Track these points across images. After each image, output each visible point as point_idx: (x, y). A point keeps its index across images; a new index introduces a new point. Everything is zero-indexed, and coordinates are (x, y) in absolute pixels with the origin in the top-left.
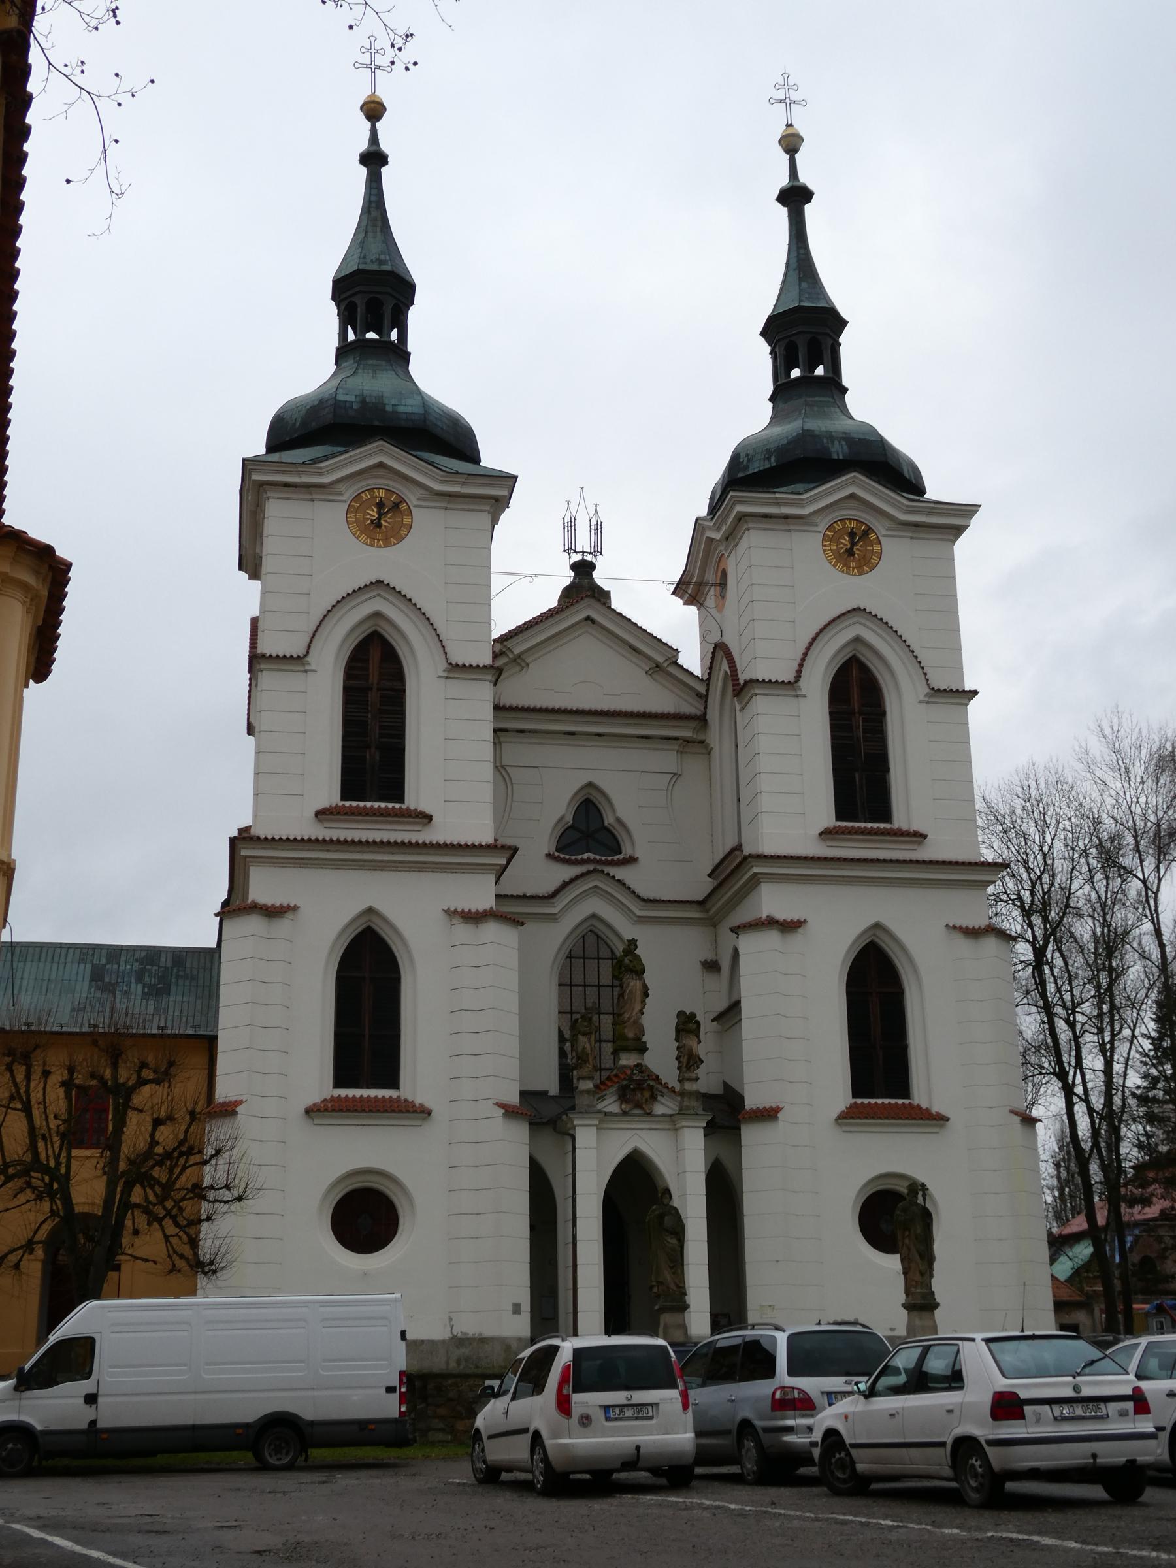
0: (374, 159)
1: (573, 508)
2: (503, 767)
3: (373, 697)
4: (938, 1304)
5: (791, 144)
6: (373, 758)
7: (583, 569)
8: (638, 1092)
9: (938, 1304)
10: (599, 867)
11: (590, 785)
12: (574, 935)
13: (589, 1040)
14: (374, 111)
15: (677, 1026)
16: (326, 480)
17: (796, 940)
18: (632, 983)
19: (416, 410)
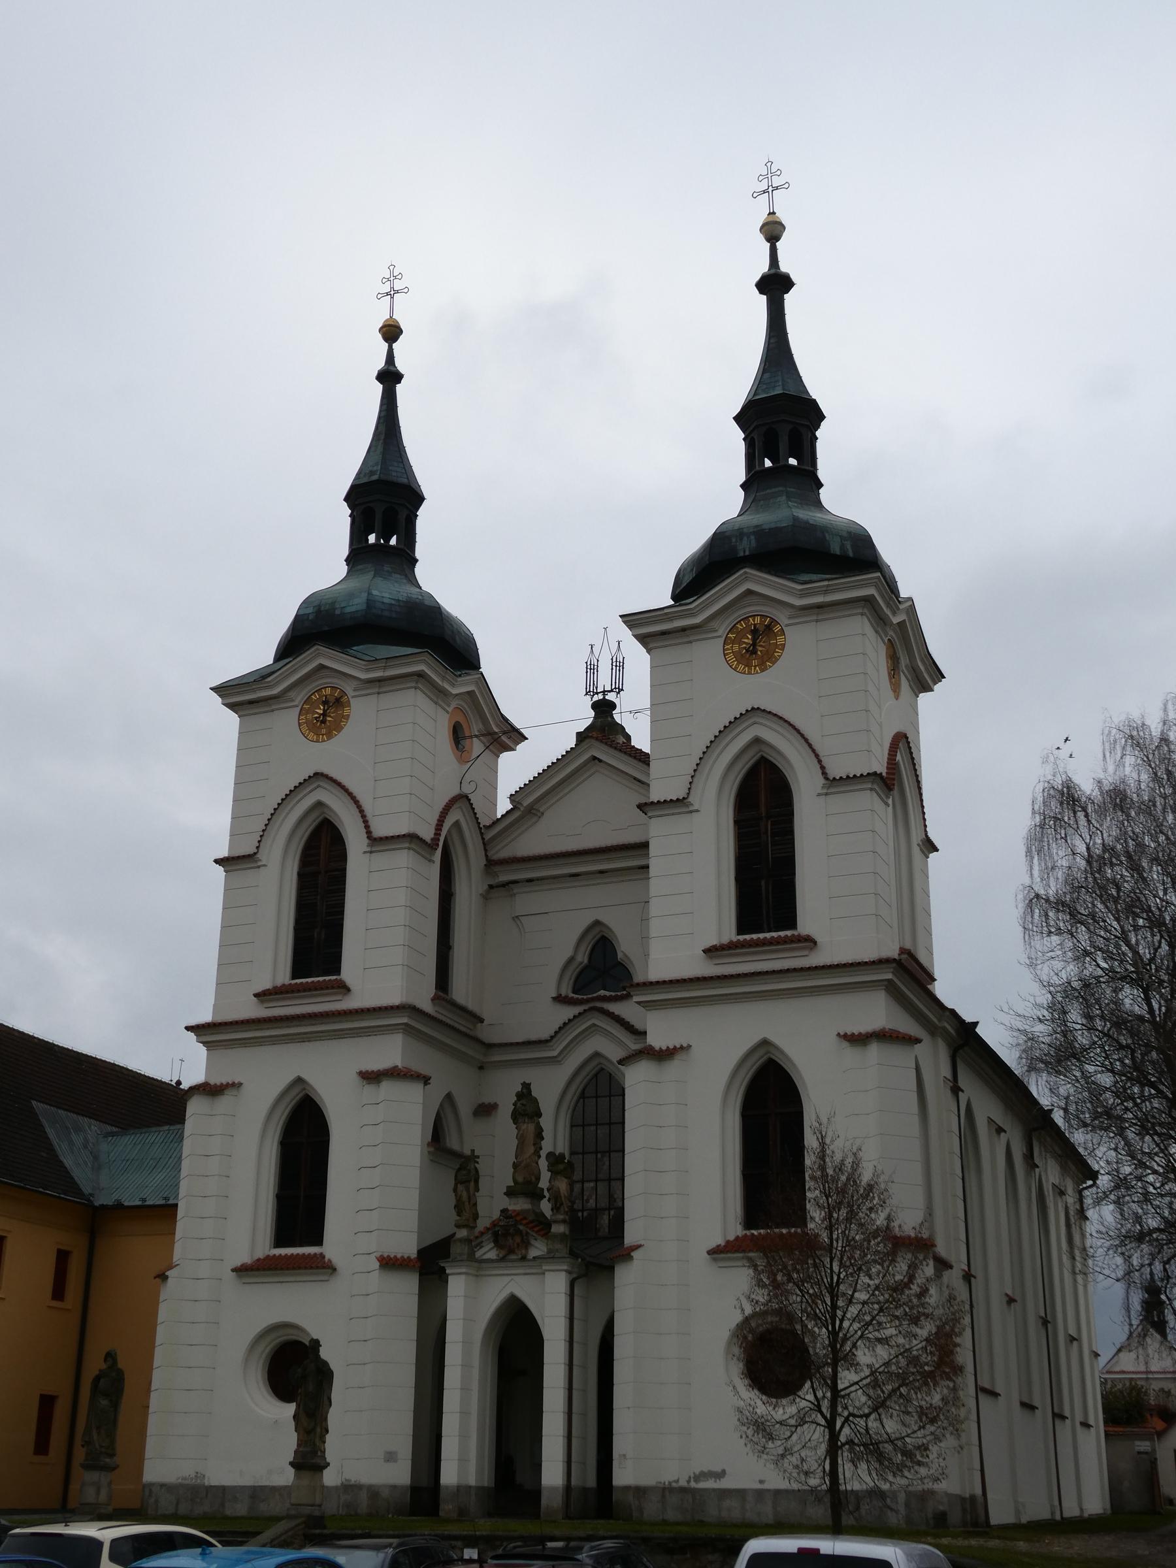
0: (390, 377)
1: (596, 650)
4: (328, 1464)
5: (773, 231)
6: (317, 938)
7: (603, 708)
8: (511, 1239)
9: (328, 1464)
10: (598, 1004)
11: (597, 923)
12: (584, 1073)
14: (391, 332)
16: (275, 691)
17: (673, 1068)
19: (359, 608)
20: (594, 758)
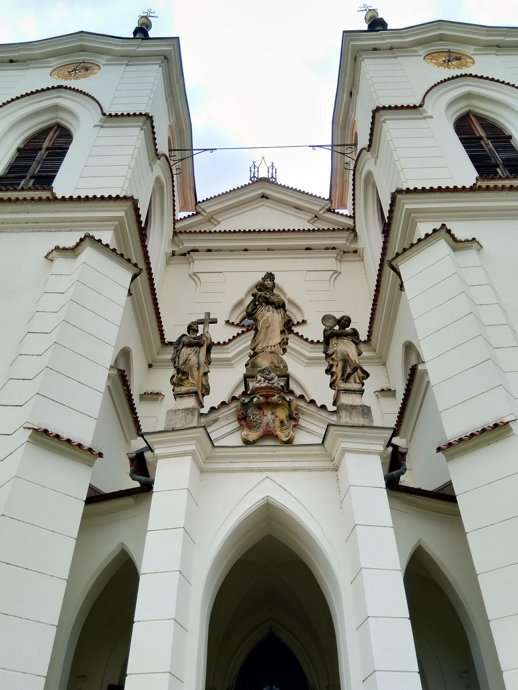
2: (194, 274)
3: (42, 154)
13: (197, 353)
15: (325, 331)
20: (264, 196)
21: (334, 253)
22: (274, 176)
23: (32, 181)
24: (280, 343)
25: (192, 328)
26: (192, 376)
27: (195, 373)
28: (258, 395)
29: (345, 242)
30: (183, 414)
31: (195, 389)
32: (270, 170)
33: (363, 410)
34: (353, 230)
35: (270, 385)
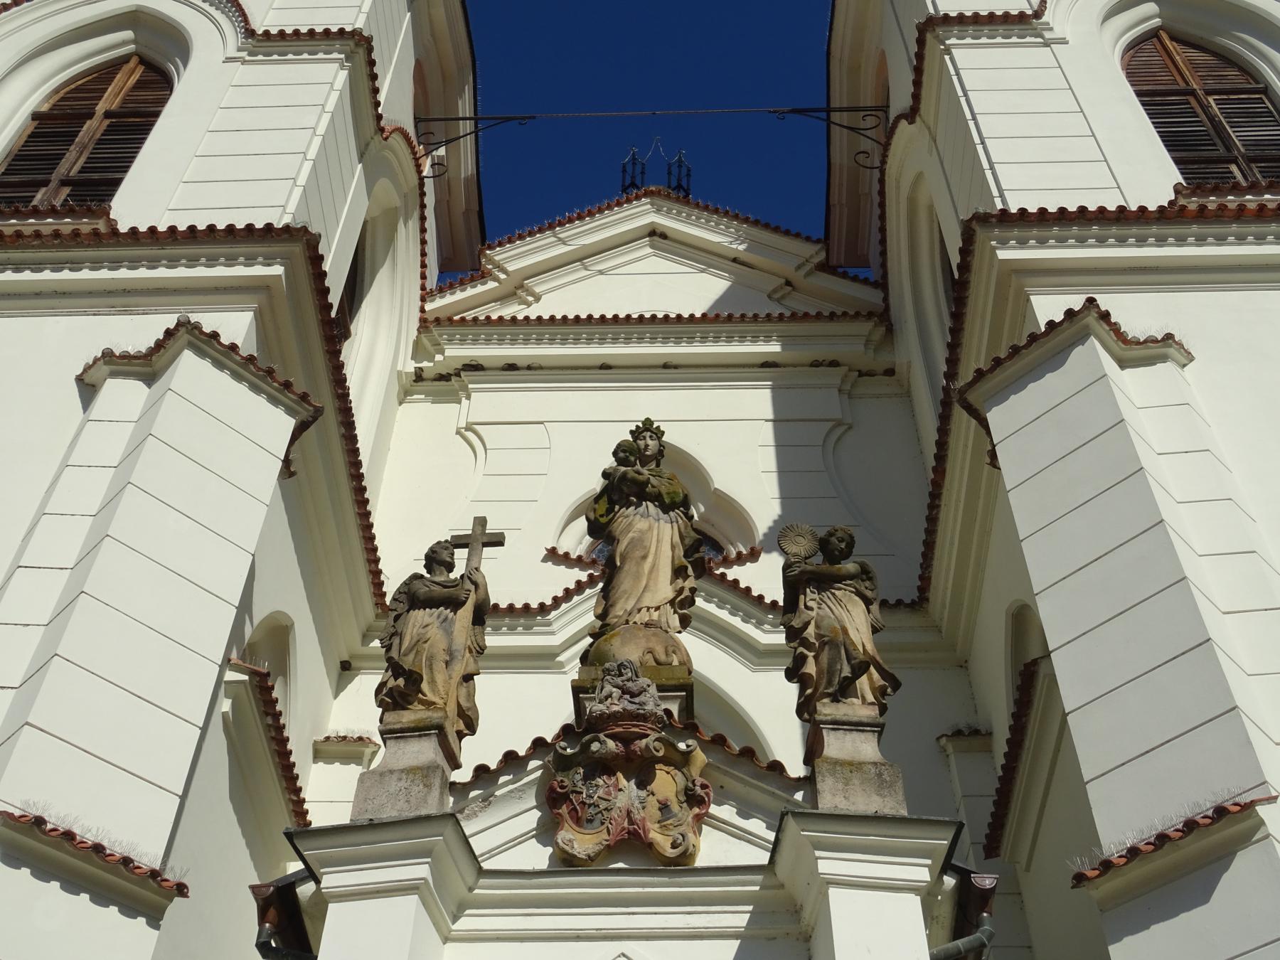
3: (92, 128)
15: (786, 568)
18: (641, 525)
21: (835, 376)
22: (684, 183)
23: (66, 191)
24: (672, 602)
25: (437, 559)
26: (433, 682)
27: (440, 678)
28: (602, 736)
29: (862, 348)
30: (403, 784)
31: (435, 716)
32: (675, 170)
33: (880, 775)
34: (883, 317)
35: (634, 707)
